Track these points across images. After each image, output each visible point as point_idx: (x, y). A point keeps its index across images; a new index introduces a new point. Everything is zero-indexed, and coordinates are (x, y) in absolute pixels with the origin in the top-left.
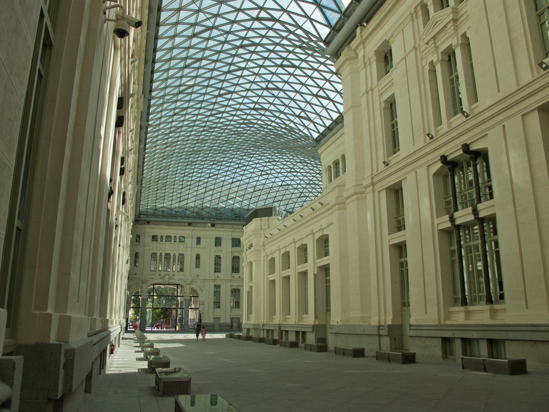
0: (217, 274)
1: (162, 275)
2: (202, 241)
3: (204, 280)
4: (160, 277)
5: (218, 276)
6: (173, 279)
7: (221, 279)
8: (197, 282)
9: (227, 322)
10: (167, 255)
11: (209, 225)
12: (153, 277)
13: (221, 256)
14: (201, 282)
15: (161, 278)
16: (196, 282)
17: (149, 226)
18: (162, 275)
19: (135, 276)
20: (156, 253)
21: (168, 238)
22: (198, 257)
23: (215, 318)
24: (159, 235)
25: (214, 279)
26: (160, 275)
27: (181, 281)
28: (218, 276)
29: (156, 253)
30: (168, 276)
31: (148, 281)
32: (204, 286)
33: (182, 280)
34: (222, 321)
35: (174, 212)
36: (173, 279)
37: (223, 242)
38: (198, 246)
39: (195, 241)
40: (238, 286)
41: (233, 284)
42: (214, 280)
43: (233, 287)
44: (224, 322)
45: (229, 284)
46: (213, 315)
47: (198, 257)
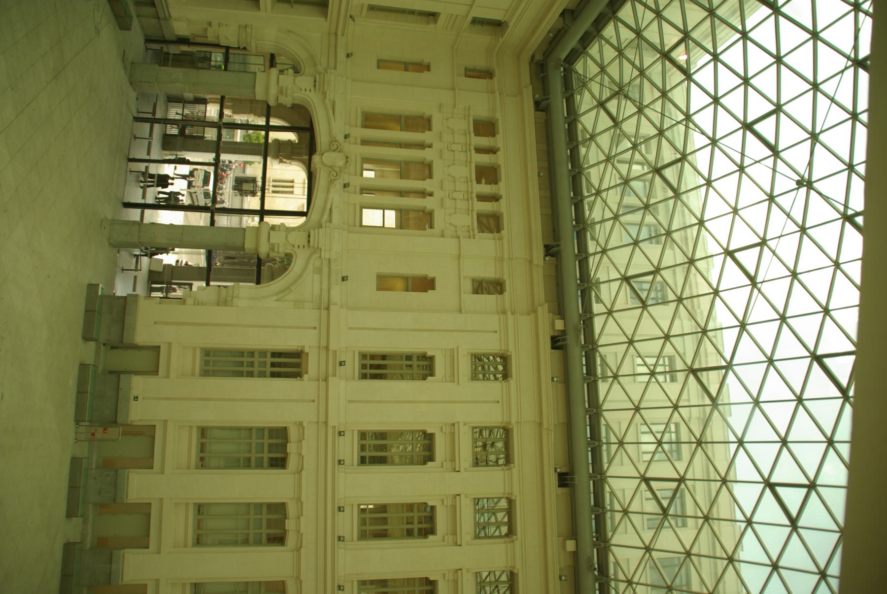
0: (353, 366)
1: (348, 147)
2: (489, 300)
3: (324, 305)
4: (340, 138)
5: (341, 364)
6: (331, 182)
7: (331, 379)
8: (317, 277)
9: (133, 404)
10: (426, 170)
11: (559, 325)
12: (337, 111)
13: (429, 378)
14: (317, 292)
15: (333, 141)
16: (319, 271)
17: (529, 106)
18: (348, 147)
19: (341, 55)
20: (430, 129)
21: (488, 174)
22: (426, 284)
23: (157, 349)
24: (499, 141)
25: (332, 347)
26: (346, 137)
27: (322, 215)
28: (341, 364)
29: (430, 129)
30: (340, 163)
31: (324, 94)
32: (299, 304)
33: (326, 217)
34: (139, 385)
35: (627, 89)
36: (331, 182)
37: (493, 388)
38: (468, 286)
39: (489, 272)
40: (300, 455)
41: (310, 432)
42: (327, 348)
43: (293, 434)
44: (134, 393)
45: (307, 414)
46: (170, 344)
47: (426, 284)
